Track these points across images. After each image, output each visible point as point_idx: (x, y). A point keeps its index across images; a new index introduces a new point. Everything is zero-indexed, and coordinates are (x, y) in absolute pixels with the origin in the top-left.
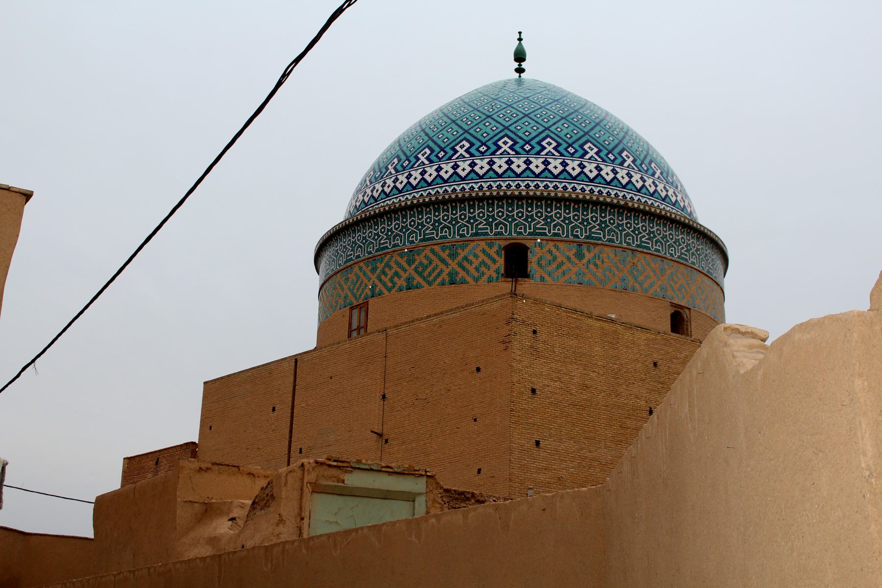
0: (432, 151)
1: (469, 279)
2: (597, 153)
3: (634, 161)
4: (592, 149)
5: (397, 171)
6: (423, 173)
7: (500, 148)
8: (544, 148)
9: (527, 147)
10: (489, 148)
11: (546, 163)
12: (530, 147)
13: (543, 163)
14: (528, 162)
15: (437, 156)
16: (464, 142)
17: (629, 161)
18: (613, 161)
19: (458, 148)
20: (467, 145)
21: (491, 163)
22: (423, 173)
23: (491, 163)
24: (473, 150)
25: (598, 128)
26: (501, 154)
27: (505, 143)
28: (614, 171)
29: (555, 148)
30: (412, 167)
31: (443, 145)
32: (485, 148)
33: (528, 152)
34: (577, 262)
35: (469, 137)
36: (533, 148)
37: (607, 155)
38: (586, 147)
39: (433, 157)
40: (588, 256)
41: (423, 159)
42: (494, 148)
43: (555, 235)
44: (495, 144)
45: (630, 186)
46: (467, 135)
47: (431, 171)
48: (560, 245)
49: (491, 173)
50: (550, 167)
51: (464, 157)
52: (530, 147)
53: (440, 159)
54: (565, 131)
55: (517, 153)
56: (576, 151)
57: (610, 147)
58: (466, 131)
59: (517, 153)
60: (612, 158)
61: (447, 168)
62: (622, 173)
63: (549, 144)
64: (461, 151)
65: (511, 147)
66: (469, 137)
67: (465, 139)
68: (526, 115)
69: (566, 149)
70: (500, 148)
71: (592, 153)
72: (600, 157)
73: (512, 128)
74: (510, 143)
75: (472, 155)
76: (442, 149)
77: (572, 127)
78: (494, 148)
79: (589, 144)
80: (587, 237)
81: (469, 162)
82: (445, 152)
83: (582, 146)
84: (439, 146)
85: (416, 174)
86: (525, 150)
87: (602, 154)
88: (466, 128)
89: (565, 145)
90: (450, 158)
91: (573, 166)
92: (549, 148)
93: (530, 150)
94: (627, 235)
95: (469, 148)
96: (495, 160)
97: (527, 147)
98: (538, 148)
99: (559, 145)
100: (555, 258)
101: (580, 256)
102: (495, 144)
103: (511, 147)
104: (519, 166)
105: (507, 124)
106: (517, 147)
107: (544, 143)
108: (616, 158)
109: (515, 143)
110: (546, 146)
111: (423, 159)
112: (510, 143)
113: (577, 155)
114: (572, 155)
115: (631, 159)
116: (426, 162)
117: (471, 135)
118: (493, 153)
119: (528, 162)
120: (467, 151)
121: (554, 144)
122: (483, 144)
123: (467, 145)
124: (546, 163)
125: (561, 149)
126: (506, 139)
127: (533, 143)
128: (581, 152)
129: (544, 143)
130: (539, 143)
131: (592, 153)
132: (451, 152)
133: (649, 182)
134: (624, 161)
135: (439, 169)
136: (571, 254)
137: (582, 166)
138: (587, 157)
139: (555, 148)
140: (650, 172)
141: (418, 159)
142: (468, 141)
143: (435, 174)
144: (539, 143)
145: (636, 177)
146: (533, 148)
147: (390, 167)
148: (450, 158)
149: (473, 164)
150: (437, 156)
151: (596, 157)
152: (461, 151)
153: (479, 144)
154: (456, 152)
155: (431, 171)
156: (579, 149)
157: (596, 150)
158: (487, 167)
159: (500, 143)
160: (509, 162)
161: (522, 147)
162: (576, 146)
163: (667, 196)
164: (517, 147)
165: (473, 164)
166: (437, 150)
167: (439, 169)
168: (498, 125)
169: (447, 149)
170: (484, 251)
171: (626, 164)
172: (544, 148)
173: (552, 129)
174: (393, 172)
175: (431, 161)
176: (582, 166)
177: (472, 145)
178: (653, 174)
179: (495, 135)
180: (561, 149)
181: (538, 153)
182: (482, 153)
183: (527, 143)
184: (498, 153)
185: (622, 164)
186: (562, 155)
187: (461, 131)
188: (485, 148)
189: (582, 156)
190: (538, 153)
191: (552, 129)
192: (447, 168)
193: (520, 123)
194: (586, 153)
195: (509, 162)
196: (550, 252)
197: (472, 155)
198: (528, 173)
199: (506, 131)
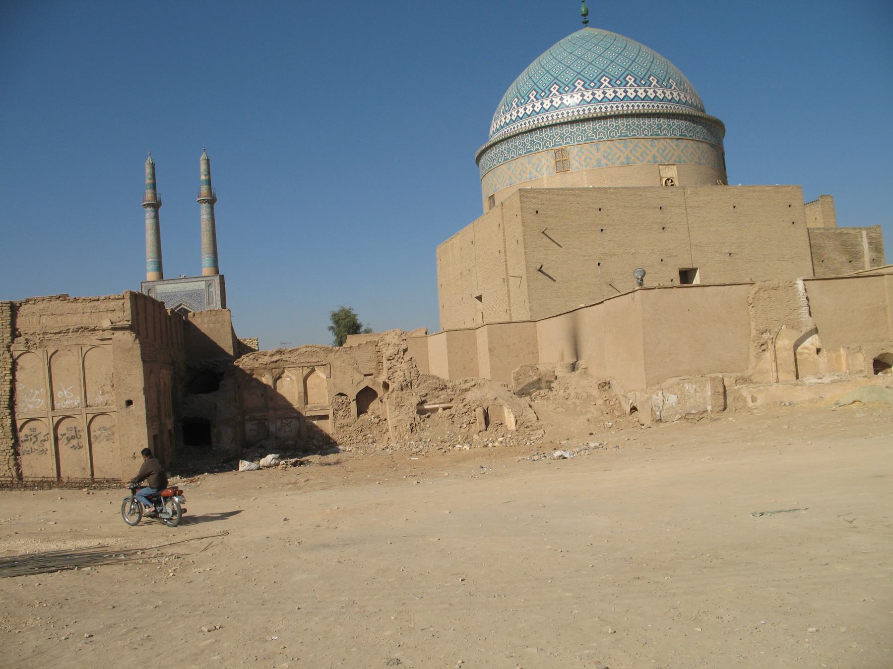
0: (537, 93)
2: (634, 82)
6: (533, 106)
7: (576, 87)
8: (602, 84)
9: (592, 85)
11: (604, 93)
14: (594, 94)
18: (644, 85)
22: (533, 106)
24: (561, 90)
28: (646, 91)
33: (593, 88)
38: (627, 79)
39: (538, 96)
41: (532, 98)
44: (573, 85)
47: (538, 106)
53: (542, 97)
58: (556, 78)
59: (586, 89)
61: (547, 103)
62: (650, 91)
63: (605, 80)
64: (554, 91)
65: (583, 86)
71: (631, 82)
74: (582, 83)
76: (543, 91)
78: (572, 88)
83: (624, 79)
85: (529, 107)
87: (637, 82)
89: (614, 80)
91: (621, 93)
92: (606, 83)
98: (598, 84)
99: (611, 80)
102: (573, 85)
106: (586, 85)
109: (585, 83)
111: (532, 98)
114: (619, 86)
119: (594, 94)
122: (567, 86)
124: (604, 93)
125: (612, 83)
127: (596, 81)
128: (624, 83)
130: (599, 81)
132: (548, 93)
133: (668, 93)
135: (542, 104)
137: (626, 92)
139: (609, 83)
143: (540, 107)
145: (659, 92)
153: (563, 86)
154: (551, 92)
160: (583, 95)
162: (621, 79)
164: (586, 85)
167: (542, 104)
172: (602, 84)
176: (626, 92)
177: (560, 87)
181: (599, 87)
183: (592, 81)
185: (650, 86)
189: (625, 86)
194: (628, 82)
197: (561, 93)
198: (594, 101)
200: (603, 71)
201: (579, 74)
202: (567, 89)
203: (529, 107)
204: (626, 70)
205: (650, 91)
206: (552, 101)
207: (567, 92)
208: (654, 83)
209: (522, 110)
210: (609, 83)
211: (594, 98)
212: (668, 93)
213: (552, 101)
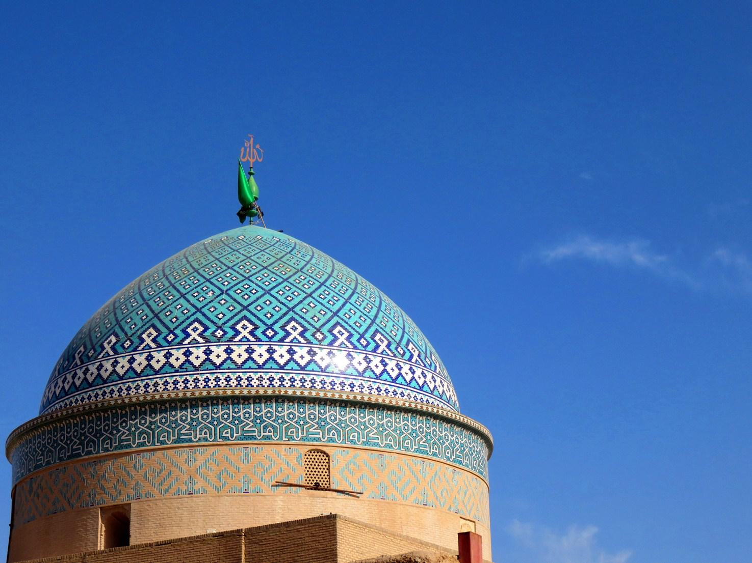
2: (348, 339)
3: (388, 346)
4: (342, 334)
5: (116, 352)
6: (149, 358)
7: (238, 333)
8: (288, 334)
10: (225, 333)
11: (291, 352)
12: (272, 333)
13: (288, 351)
14: (271, 351)
15: (165, 339)
16: (196, 324)
17: (383, 346)
19: (189, 330)
20: (201, 329)
21: (229, 351)
22: (149, 358)
23: (229, 351)
26: (240, 341)
27: (244, 327)
30: (135, 350)
31: (172, 327)
32: (222, 333)
33: (270, 338)
36: (276, 333)
37: (358, 340)
38: (335, 332)
41: (148, 341)
44: (233, 328)
45: (385, 376)
46: (199, 316)
47: (159, 356)
49: (229, 362)
50: (296, 357)
51: (198, 343)
52: (272, 333)
55: (259, 340)
56: (325, 337)
57: (361, 331)
58: (198, 310)
60: (365, 343)
61: (178, 355)
63: (295, 329)
64: (194, 335)
65: (251, 333)
67: (197, 320)
69: (313, 335)
70: (238, 333)
71: (342, 339)
72: (352, 343)
74: (251, 327)
75: (207, 341)
77: (319, 307)
78: (231, 333)
79: (339, 328)
81: (204, 348)
82: (174, 334)
83: (330, 331)
84: (167, 328)
85: (141, 359)
86: (267, 336)
87: (354, 340)
88: (199, 305)
89: (312, 330)
90: (180, 343)
92: (295, 334)
93: (273, 336)
96: (232, 347)
97: (270, 333)
98: (282, 334)
102: (233, 328)
103: (251, 333)
104: (261, 355)
106: (258, 333)
107: (288, 328)
108: (368, 344)
110: (291, 331)
111: (148, 341)
112: (251, 327)
113: (326, 342)
114: (320, 341)
115: (386, 342)
116: (153, 345)
117: (204, 315)
118: (231, 340)
119: (271, 351)
120: (200, 335)
121: (300, 329)
123: (201, 329)
124: (291, 352)
126: (245, 322)
127: (276, 327)
128: (330, 338)
129: (288, 328)
130: (283, 328)
131: (342, 339)
132: (182, 336)
133: (406, 368)
134: (378, 346)
135: (168, 355)
138: (337, 344)
140: (408, 355)
141: (143, 341)
142: (201, 323)
144: (283, 328)
146: (276, 333)
147: (105, 344)
148: (180, 343)
149: (208, 352)
150: (165, 339)
151: (347, 343)
152: (194, 335)
153: (212, 328)
154: (188, 335)
155: (159, 356)
156: (327, 334)
157: (346, 334)
159: (239, 327)
160: (250, 351)
161: (264, 333)
162: (325, 330)
164: (258, 333)
165: (208, 352)
166: (165, 331)
167: (168, 355)
168: (236, 305)
169: (178, 332)
171: (379, 351)
172: (288, 334)
174: (111, 353)
175: (159, 346)
182: (219, 340)
183: (270, 327)
184: (237, 339)
185: (375, 350)
186: (309, 342)
187: (193, 310)
188: (222, 333)
189: (331, 344)
190: (282, 340)
191: (297, 309)
192: (178, 355)
193: (260, 302)
194: (336, 338)
195: (250, 351)
197: (207, 341)
199: (245, 313)
201: (245, 308)
202: (219, 333)
203: (141, 359)
204: (335, 314)
205: (376, 361)
206: (187, 353)
207: (219, 340)
208: (383, 346)
209: (123, 362)
210: (302, 334)
212: (406, 368)
213: (187, 353)
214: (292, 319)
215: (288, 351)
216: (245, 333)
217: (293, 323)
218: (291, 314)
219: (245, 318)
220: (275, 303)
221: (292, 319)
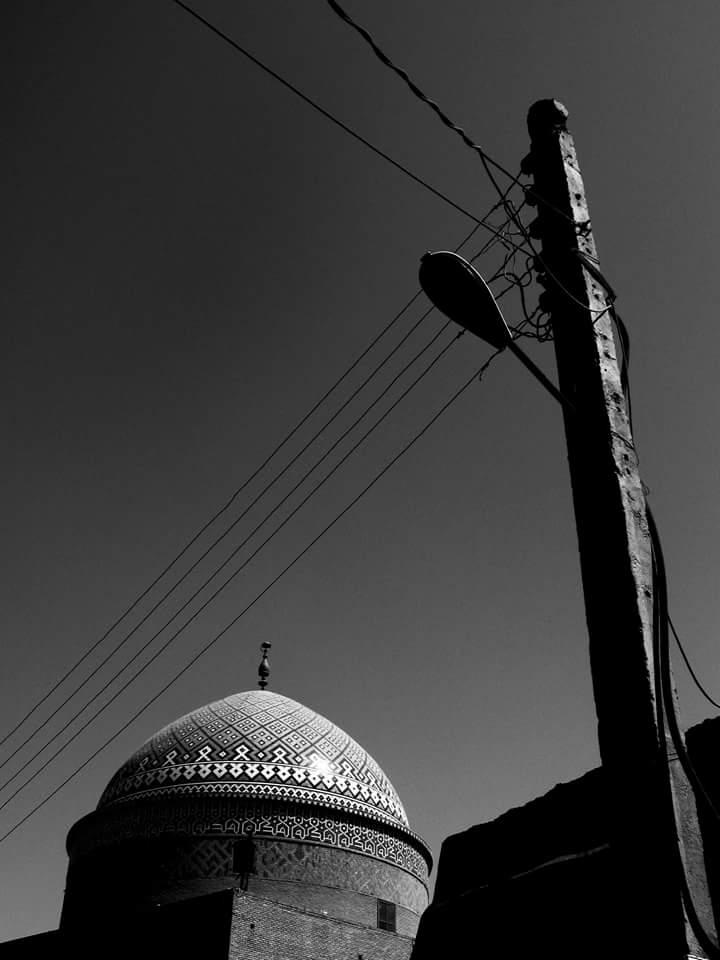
1: (201, 873)
3: (352, 771)
8: (275, 756)
9: (261, 755)
11: (276, 770)
13: (273, 770)
14: (260, 768)
16: (207, 747)
17: (348, 771)
19: (201, 752)
20: (209, 750)
21: (229, 767)
23: (229, 767)
24: (213, 755)
25: (323, 740)
27: (242, 750)
29: (285, 757)
30: (160, 766)
33: (261, 759)
34: (296, 859)
35: (211, 743)
40: (307, 855)
42: (232, 754)
43: (279, 834)
44: (234, 750)
45: (348, 793)
48: (283, 844)
51: (205, 760)
53: (185, 761)
54: (295, 742)
55: (252, 760)
58: (210, 738)
59: (252, 760)
63: (280, 753)
64: (204, 755)
66: (211, 743)
68: (262, 726)
69: (294, 758)
73: (249, 737)
74: (247, 750)
76: (188, 753)
77: (301, 739)
78: (232, 754)
80: (306, 838)
81: (209, 766)
84: (185, 750)
88: (210, 734)
89: (294, 754)
92: (280, 757)
94: (343, 837)
95: (211, 753)
96: (233, 765)
97: (261, 755)
98: (270, 756)
100: (278, 857)
101: (300, 855)
105: (245, 734)
107: (275, 752)
109: (251, 750)
112: (247, 750)
118: (231, 759)
119: (260, 768)
120: (208, 755)
121: (284, 753)
123: (209, 750)
124: (276, 770)
125: (289, 758)
126: (243, 746)
127: (266, 751)
129: (275, 752)
133: (364, 789)
136: (292, 853)
139: (285, 757)
140: (366, 780)
142: (210, 746)
144: (271, 752)
145: (353, 785)
148: (193, 761)
149: (213, 768)
150: (182, 758)
152: (204, 755)
153: (219, 749)
158: (225, 771)
159: (238, 750)
160: (244, 768)
163: (380, 802)
165: (213, 768)
166: (183, 752)
170: (215, 847)
171: (345, 773)
172: (275, 756)
173: (283, 740)
177: (214, 750)
178: (368, 783)
179: (235, 742)
180: (289, 758)
181: (270, 761)
182: (222, 758)
183: (261, 751)
186: (290, 763)
187: (205, 738)
190: (270, 761)
191: (283, 740)
195: (244, 768)
196: (274, 850)
197: (213, 759)
200: (279, 739)
202: (223, 754)
204: (312, 745)
208: (348, 771)
211: (260, 774)
214: (279, 746)
215: (273, 770)
216: (242, 754)
217: (280, 749)
218: (279, 742)
219: (243, 743)
220: (268, 734)
221: (279, 746)
